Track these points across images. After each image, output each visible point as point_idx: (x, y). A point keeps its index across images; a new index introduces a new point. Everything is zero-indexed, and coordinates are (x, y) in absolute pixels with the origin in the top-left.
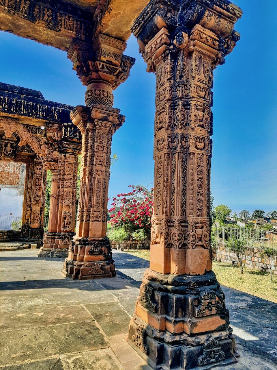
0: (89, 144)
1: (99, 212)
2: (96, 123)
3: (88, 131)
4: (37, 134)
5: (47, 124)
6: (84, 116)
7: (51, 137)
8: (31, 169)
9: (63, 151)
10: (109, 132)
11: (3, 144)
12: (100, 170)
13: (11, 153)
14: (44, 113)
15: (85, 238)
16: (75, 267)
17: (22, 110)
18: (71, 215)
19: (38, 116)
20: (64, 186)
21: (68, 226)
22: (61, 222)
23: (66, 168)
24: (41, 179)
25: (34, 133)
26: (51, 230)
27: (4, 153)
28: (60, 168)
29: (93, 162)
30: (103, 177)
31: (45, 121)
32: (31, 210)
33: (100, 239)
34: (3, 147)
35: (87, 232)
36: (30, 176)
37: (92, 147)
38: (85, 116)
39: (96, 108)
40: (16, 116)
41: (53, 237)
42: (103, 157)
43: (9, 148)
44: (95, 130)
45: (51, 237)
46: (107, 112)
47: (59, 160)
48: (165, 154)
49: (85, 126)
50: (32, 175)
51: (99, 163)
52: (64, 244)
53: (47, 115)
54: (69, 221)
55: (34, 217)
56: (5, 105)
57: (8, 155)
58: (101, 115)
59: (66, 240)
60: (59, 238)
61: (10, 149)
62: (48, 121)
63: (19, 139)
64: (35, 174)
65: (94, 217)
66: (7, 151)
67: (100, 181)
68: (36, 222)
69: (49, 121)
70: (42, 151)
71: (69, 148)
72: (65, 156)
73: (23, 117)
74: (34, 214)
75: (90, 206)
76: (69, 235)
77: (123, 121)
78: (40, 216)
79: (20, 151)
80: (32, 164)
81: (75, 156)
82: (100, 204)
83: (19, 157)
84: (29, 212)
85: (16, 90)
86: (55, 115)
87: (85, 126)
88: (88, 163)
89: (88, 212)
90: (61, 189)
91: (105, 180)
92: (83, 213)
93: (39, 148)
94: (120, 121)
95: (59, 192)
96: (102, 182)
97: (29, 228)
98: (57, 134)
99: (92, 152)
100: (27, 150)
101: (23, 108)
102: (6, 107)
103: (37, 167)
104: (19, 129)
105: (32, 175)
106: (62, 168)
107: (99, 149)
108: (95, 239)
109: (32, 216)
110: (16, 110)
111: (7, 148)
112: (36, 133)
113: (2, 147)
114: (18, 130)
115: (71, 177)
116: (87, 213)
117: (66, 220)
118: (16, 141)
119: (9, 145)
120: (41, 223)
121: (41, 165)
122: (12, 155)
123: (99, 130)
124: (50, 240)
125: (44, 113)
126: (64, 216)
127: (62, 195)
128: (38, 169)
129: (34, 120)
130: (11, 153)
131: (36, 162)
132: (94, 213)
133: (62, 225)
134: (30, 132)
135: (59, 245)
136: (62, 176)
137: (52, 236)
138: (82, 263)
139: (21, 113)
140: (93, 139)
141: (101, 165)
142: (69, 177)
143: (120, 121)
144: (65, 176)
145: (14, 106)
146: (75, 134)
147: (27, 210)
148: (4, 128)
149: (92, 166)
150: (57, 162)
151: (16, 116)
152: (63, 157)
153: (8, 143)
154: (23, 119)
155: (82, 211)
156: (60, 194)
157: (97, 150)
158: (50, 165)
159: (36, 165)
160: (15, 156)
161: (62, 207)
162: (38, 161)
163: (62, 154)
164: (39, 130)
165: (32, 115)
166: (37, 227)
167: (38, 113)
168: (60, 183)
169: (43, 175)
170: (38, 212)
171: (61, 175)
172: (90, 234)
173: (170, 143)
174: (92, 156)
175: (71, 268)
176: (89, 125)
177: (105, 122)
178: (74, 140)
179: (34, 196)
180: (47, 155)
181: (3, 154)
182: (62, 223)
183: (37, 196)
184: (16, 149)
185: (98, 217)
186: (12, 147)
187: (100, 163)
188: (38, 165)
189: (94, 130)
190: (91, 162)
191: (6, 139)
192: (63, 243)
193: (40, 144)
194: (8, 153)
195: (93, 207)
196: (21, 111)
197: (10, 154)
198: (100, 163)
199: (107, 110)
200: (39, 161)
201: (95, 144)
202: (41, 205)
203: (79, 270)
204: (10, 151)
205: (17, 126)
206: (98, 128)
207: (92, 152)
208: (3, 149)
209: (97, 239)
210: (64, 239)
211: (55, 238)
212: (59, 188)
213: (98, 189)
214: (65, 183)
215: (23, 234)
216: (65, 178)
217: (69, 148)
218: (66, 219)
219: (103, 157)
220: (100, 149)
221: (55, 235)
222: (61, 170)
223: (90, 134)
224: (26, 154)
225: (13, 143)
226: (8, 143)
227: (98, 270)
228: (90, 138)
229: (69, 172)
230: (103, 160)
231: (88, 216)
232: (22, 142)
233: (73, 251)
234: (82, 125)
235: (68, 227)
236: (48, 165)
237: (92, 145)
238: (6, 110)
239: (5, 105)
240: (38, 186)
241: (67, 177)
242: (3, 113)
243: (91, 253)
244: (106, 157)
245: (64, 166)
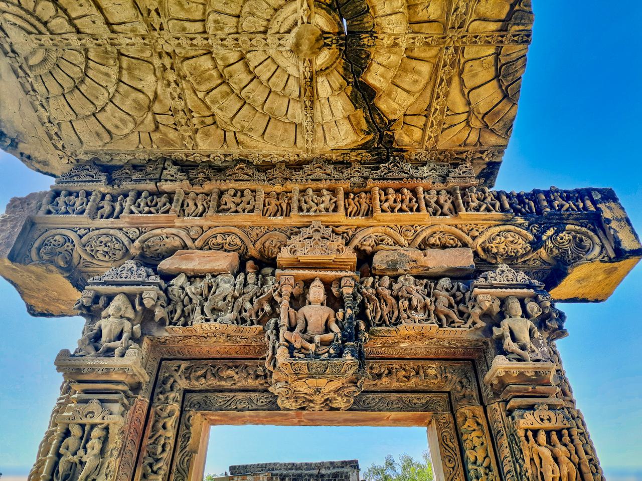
4: (463, 212)
8: (480, 454)
11: (280, 295)
13: (330, 336)
27: (291, 349)
34: (284, 308)
61: (327, 311)
66: (304, 331)
79: (382, 322)
80: (479, 410)
83: (379, 376)
103: (529, 420)
111: (306, 310)
112: (455, 210)
113: (278, 316)
119: (316, 292)
122: (339, 355)
128: (542, 437)
130: (330, 336)
134: (418, 210)
153: (308, 283)
159: (510, 412)
164: (463, 195)
181: (282, 354)
184: (362, 315)
186: (334, 301)
188: (531, 408)
191: (298, 265)
197: (329, 343)
200: (528, 367)
208: (284, 320)
224: (420, 348)
225: (340, 280)
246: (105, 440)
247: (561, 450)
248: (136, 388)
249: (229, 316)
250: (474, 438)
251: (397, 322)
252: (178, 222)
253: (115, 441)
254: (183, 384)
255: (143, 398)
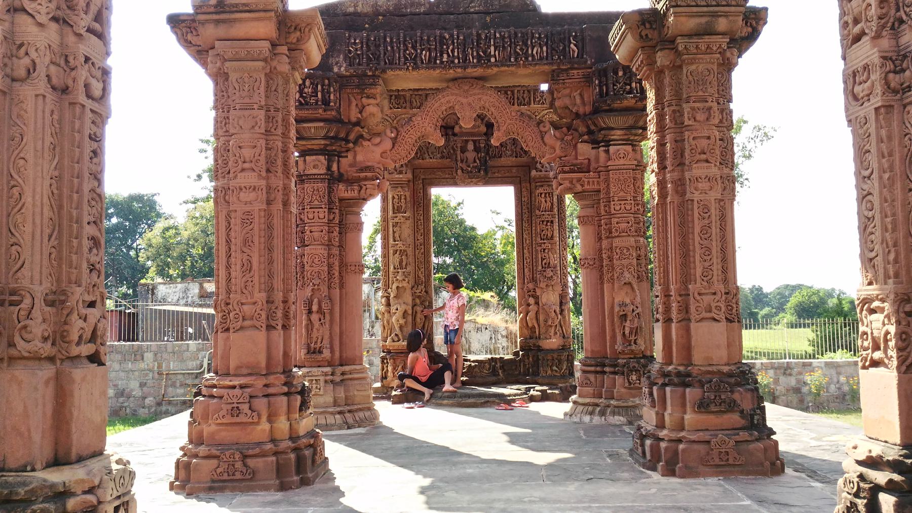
0: (666, 109)
1: (715, 294)
2: (680, 49)
3: (661, 72)
4: (532, 105)
5: (553, 78)
6: (646, 35)
7: (567, 108)
9: (598, 140)
10: (719, 65)
12: (703, 177)
14: (545, 48)
15: (681, 368)
16: (663, 445)
17: (492, 53)
18: (639, 310)
19: (530, 59)
20: (610, 233)
21: (633, 338)
22: (613, 330)
23: (611, 185)
24: (552, 222)
25: (524, 105)
26: (592, 351)
27: (462, 169)
28: (596, 187)
29: (682, 157)
30: (714, 195)
31: (547, 68)
32: (537, 303)
33: (726, 369)
35: (687, 349)
36: (525, 216)
37: (678, 115)
38: (650, 36)
39: (677, 6)
40: (479, 71)
41: (598, 369)
42: (709, 138)
43: (471, 155)
44: (680, 67)
45: (592, 369)
46: (711, 9)
47: (593, 165)
48: (877, 109)
49: (651, 63)
50: (531, 212)
51: (698, 157)
52: (630, 389)
53: (552, 50)
54: (635, 325)
55: (546, 321)
56: (453, 51)
57: (471, 172)
58: (692, 24)
59: (634, 377)
60: (615, 373)
62: (555, 67)
63: (490, 126)
64: (537, 211)
65: (699, 309)
67: (706, 209)
68: (552, 334)
69: (559, 65)
70: (548, 149)
71: (613, 129)
72: (607, 152)
73: (495, 69)
74: (547, 314)
75: (686, 279)
76: (638, 363)
77: (761, 22)
78: (560, 316)
81: (633, 145)
82: (715, 273)
84: (533, 308)
85: (473, 7)
86: (572, 46)
87: (651, 63)
88: (668, 163)
89: (680, 295)
90: (605, 243)
91: (722, 203)
92: (668, 300)
93: (540, 139)
94: (751, 26)
95: (600, 250)
96: (713, 210)
97: (539, 349)
98: (580, 94)
99: (678, 130)
100: (512, 150)
101: (492, 48)
102: (456, 54)
103: (541, 190)
104: (488, 101)
105: (531, 212)
106: (602, 186)
107: (698, 118)
108: (710, 369)
109: (541, 318)
110: (479, 58)
111: (467, 154)
114: (487, 105)
115: (628, 207)
116: (679, 299)
117: (628, 324)
118: (485, 134)
120: (564, 337)
121: (549, 186)
123: (692, 64)
124: (592, 377)
125: (545, 48)
126: (622, 313)
127: (611, 259)
129: (522, 71)
131: (534, 179)
132: (698, 298)
133: (619, 338)
135: (615, 391)
136: (605, 206)
137: (597, 366)
138: (682, 434)
139: (490, 61)
140: (678, 96)
141: (707, 161)
142: (623, 206)
143: (751, 26)
144: (612, 207)
145: (472, 49)
146: (628, 87)
147: (529, 305)
148: (457, 107)
149: (680, 168)
150: (589, 172)
151: (479, 71)
152: (602, 155)
153: (467, 141)
154: (496, 75)
155: (665, 296)
156: (604, 256)
157: (691, 123)
158: (571, 182)
160: (486, 171)
161: (613, 288)
162: (540, 177)
163: (598, 148)
164: (534, 94)
165: (516, 59)
166: (555, 347)
167: (530, 52)
168: (600, 226)
169: (556, 210)
170: (554, 307)
171: (602, 205)
172: (698, 357)
173: (891, 75)
174: (679, 142)
175: (651, 446)
176: (662, 58)
177: (707, 39)
178: (626, 103)
179: (540, 268)
180: (560, 158)
181: (459, 171)
182: (617, 331)
183: (549, 267)
184: (487, 153)
185: (714, 310)
186: (477, 149)
187: (704, 157)
189: (677, 68)
190: (674, 159)
192: (627, 385)
193: (541, 132)
194: (469, 166)
195: (695, 281)
196: (490, 56)
197: (476, 167)
198: (704, 157)
199: (707, 6)
200: (543, 173)
201: (684, 105)
202: (559, 289)
203: (676, 452)
204: (475, 162)
205: (485, 98)
206: (688, 59)
207: (678, 130)
208: (459, 158)
209: (714, 369)
210: (628, 376)
211: (604, 373)
212: (600, 239)
213: (706, 229)
214: (614, 224)
215: (524, 365)
216: (613, 212)
217: (613, 129)
218: (628, 322)
219: (709, 138)
220: (700, 117)
221: (603, 365)
222: (599, 191)
223: (667, 80)
226: (467, 141)
227: (727, 453)
228: (667, 93)
229: (622, 194)
230: (711, 147)
231: (685, 309)
232: (500, 134)
233: (653, 401)
234: (642, 62)
235: (635, 343)
236: (567, 184)
237: (674, 111)
238: (456, 61)
239: (453, 51)
240: (547, 239)
241: (618, 208)
242: (451, 71)
243: (702, 406)
244: (718, 138)
245: (607, 181)
246: (405, 199)
247: (548, 199)
248: (409, 181)
249: (439, 156)
250: (525, 194)
251: (501, 157)
252: (411, 112)
253: (408, 199)
254: (423, 177)
255: (411, 184)
